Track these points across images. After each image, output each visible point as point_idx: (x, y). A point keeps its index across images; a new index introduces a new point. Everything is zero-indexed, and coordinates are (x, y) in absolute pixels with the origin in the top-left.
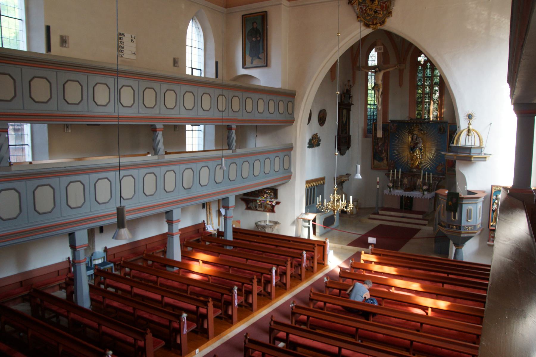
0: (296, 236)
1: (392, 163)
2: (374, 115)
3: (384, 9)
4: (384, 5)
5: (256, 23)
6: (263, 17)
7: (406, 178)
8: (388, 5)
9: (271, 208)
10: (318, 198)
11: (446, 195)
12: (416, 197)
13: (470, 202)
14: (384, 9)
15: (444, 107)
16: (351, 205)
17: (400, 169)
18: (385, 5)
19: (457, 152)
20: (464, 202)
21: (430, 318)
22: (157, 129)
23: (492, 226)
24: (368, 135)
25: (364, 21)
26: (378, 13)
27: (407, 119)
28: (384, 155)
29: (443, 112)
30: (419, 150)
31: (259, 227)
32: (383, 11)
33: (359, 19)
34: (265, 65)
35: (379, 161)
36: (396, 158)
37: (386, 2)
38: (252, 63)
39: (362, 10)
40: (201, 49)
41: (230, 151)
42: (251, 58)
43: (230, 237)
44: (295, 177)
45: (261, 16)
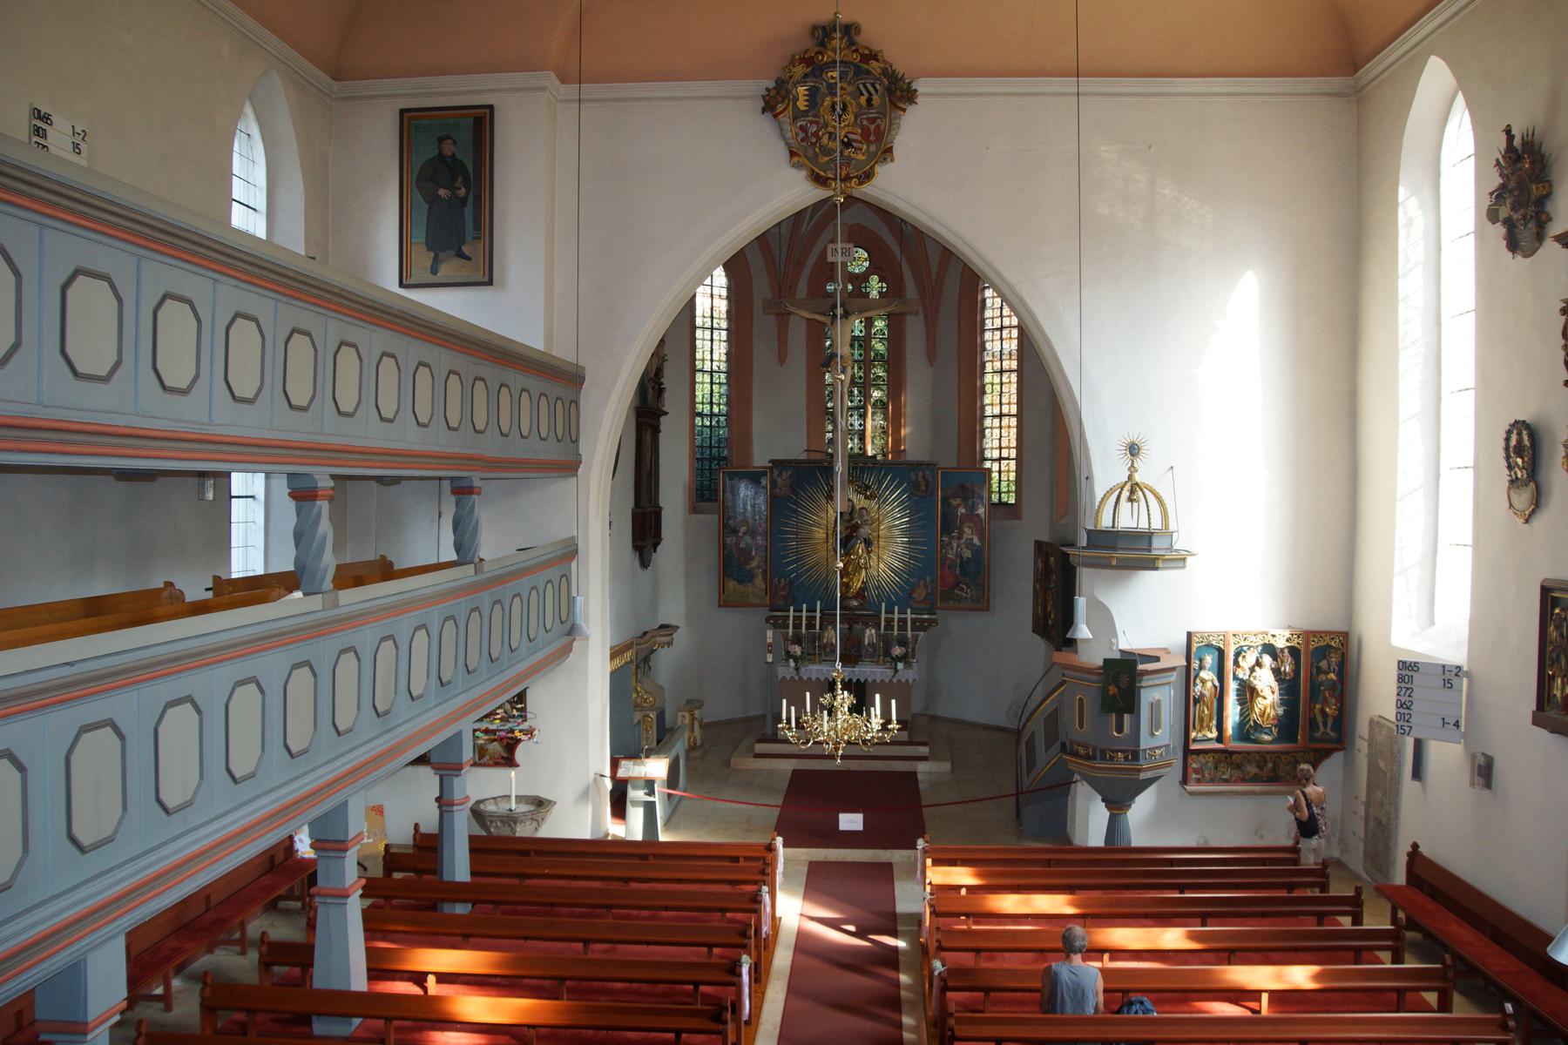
0: (594, 838)
1: (782, 585)
2: (711, 446)
3: (872, 138)
4: (873, 127)
5: (451, 141)
6: (481, 122)
7: (830, 627)
8: (882, 128)
9: (506, 755)
10: (872, 709)
11: (1100, 668)
12: (874, 680)
13: (1157, 682)
14: (872, 138)
15: (905, 422)
16: (894, 725)
17: (819, 603)
19: (1114, 548)
20: (1144, 684)
21: (1266, 1021)
22: (319, 493)
23: (1195, 740)
24: (700, 504)
25: (811, 165)
26: (853, 147)
27: (804, 457)
28: (754, 564)
29: (905, 436)
30: (863, 544)
31: (491, 822)
32: (869, 143)
33: (796, 159)
34: (486, 279)
35: (740, 582)
36: (792, 571)
37: (879, 118)
38: (434, 271)
40: (255, 210)
41: (469, 570)
42: (432, 254)
43: (459, 867)
44: (586, 648)
45: (472, 119)
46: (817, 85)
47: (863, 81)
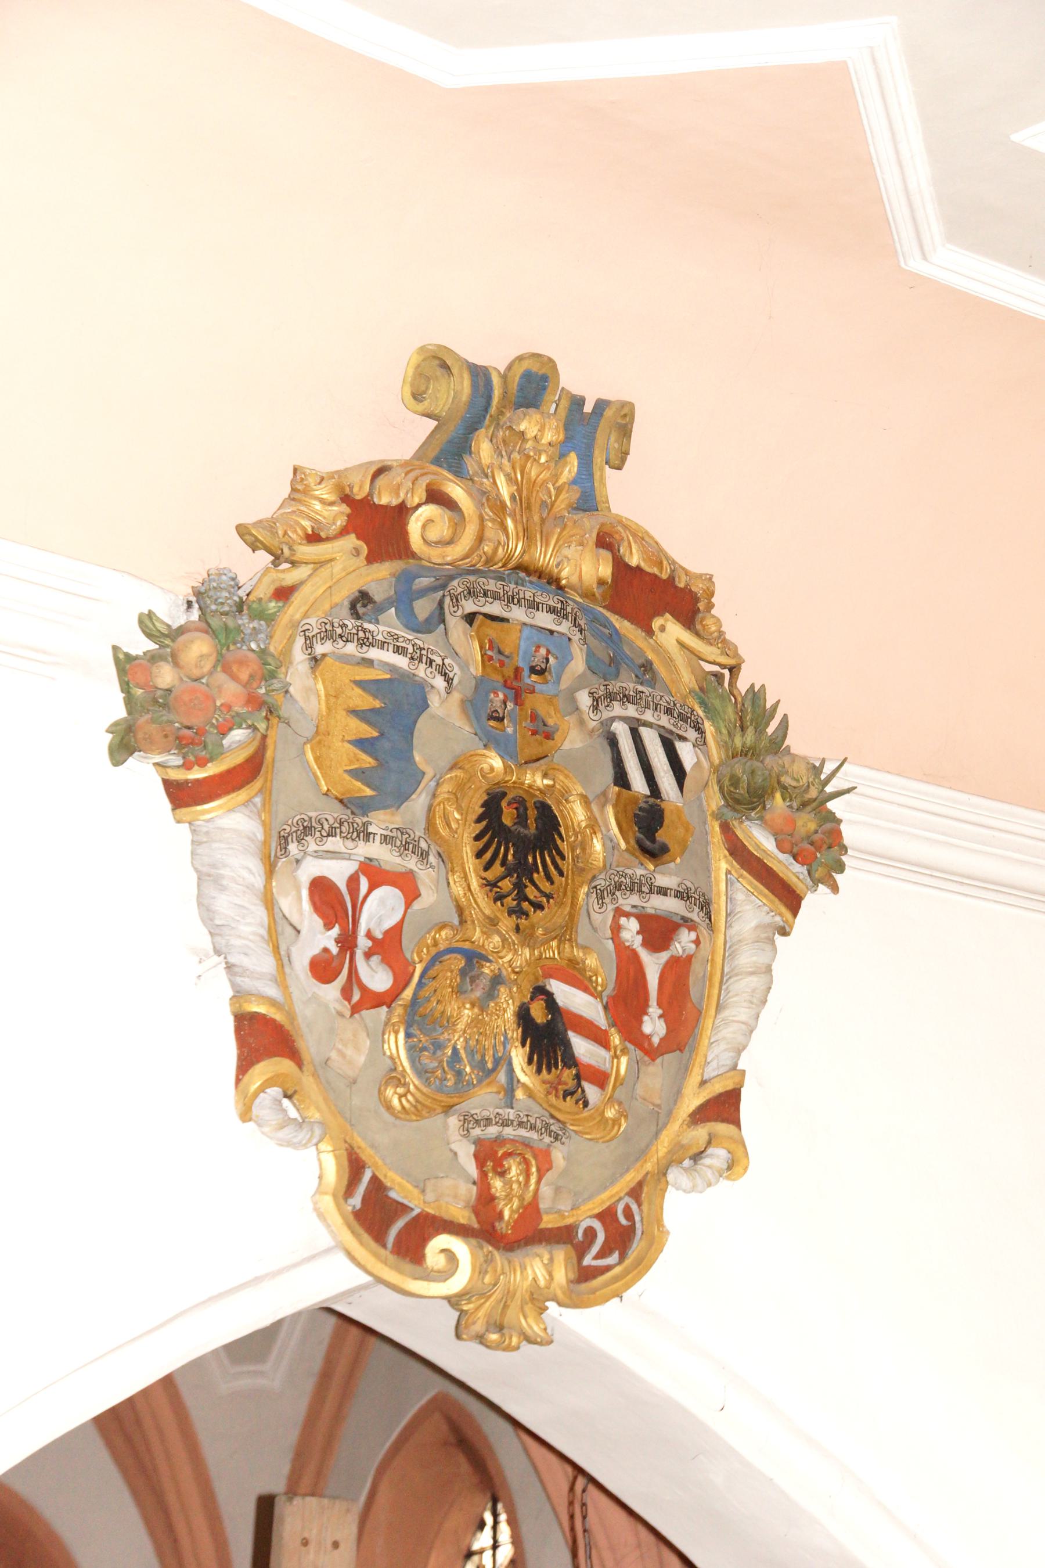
3: (654, 1026)
18: (664, 956)
39: (347, 942)
46: (422, 671)
47: (631, 711)
